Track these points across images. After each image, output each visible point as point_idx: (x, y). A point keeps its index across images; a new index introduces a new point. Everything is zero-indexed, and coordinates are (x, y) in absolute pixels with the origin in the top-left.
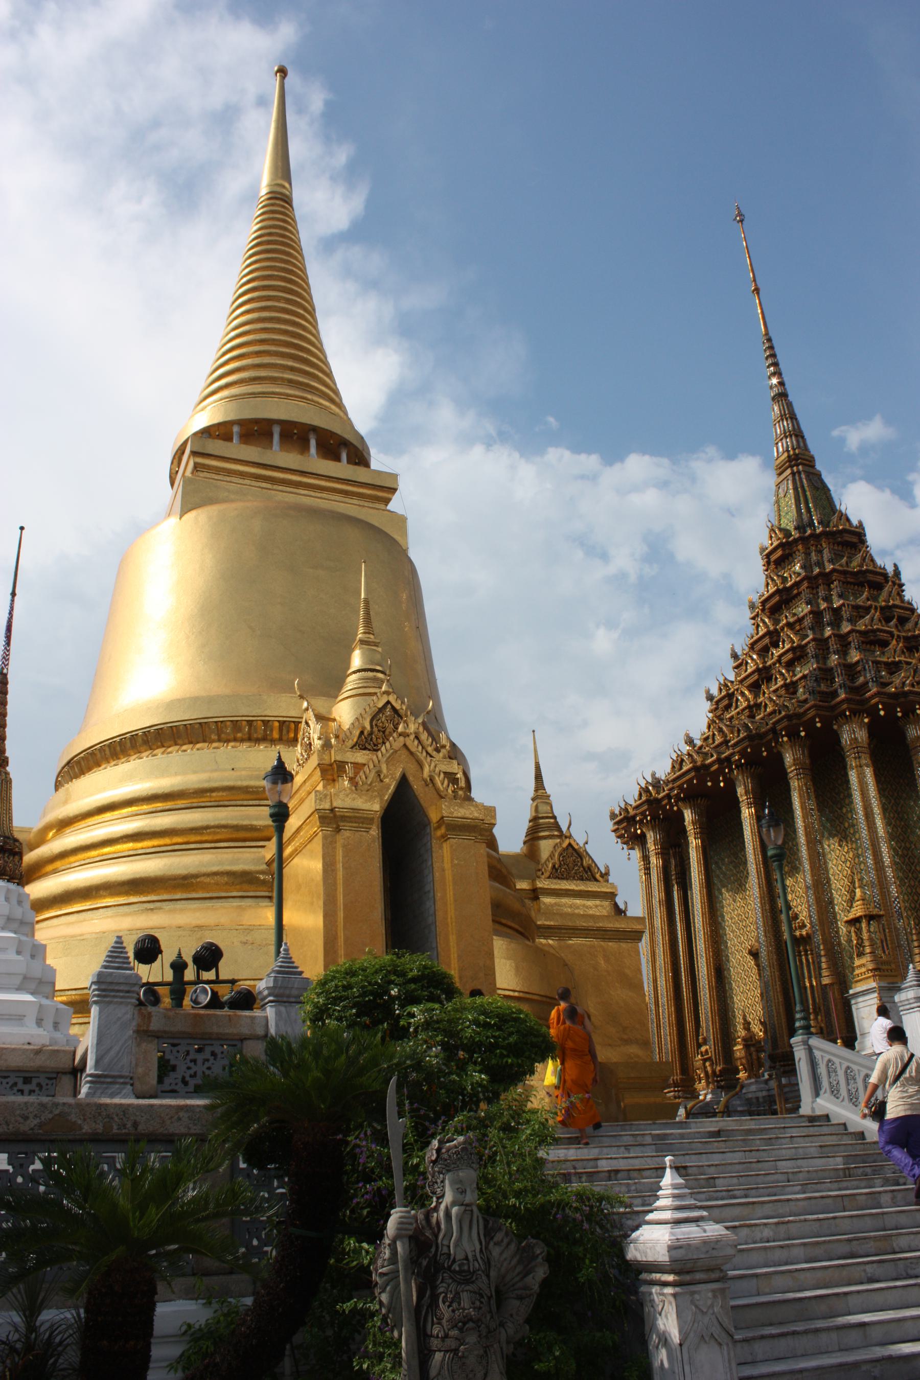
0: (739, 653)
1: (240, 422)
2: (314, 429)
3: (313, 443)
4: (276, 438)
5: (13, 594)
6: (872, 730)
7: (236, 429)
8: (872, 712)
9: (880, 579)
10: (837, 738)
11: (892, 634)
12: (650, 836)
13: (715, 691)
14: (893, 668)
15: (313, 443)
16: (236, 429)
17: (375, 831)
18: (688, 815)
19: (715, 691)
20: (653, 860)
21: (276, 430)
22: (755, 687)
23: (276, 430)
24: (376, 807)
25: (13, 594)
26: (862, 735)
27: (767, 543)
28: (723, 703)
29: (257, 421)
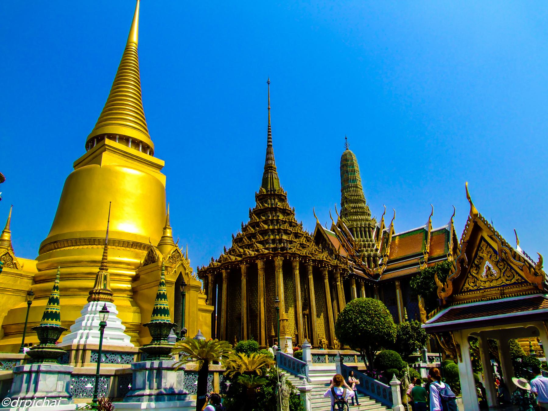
0: (244, 225)
1: (120, 135)
2: (141, 142)
3: (141, 146)
4: (130, 143)
5: (108, 222)
6: (284, 261)
7: (118, 137)
8: (285, 257)
9: (289, 212)
10: (274, 262)
11: (291, 232)
12: (210, 278)
13: (235, 236)
14: (291, 242)
15: (141, 146)
16: (118, 137)
17: (174, 286)
18: (224, 275)
19: (235, 236)
20: (210, 285)
21: (131, 140)
22: (250, 238)
23: (131, 140)
24: (174, 280)
25: (108, 222)
26: (281, 263)
27: (258, 193)
28: (238, 240)
29: (125, 136)
